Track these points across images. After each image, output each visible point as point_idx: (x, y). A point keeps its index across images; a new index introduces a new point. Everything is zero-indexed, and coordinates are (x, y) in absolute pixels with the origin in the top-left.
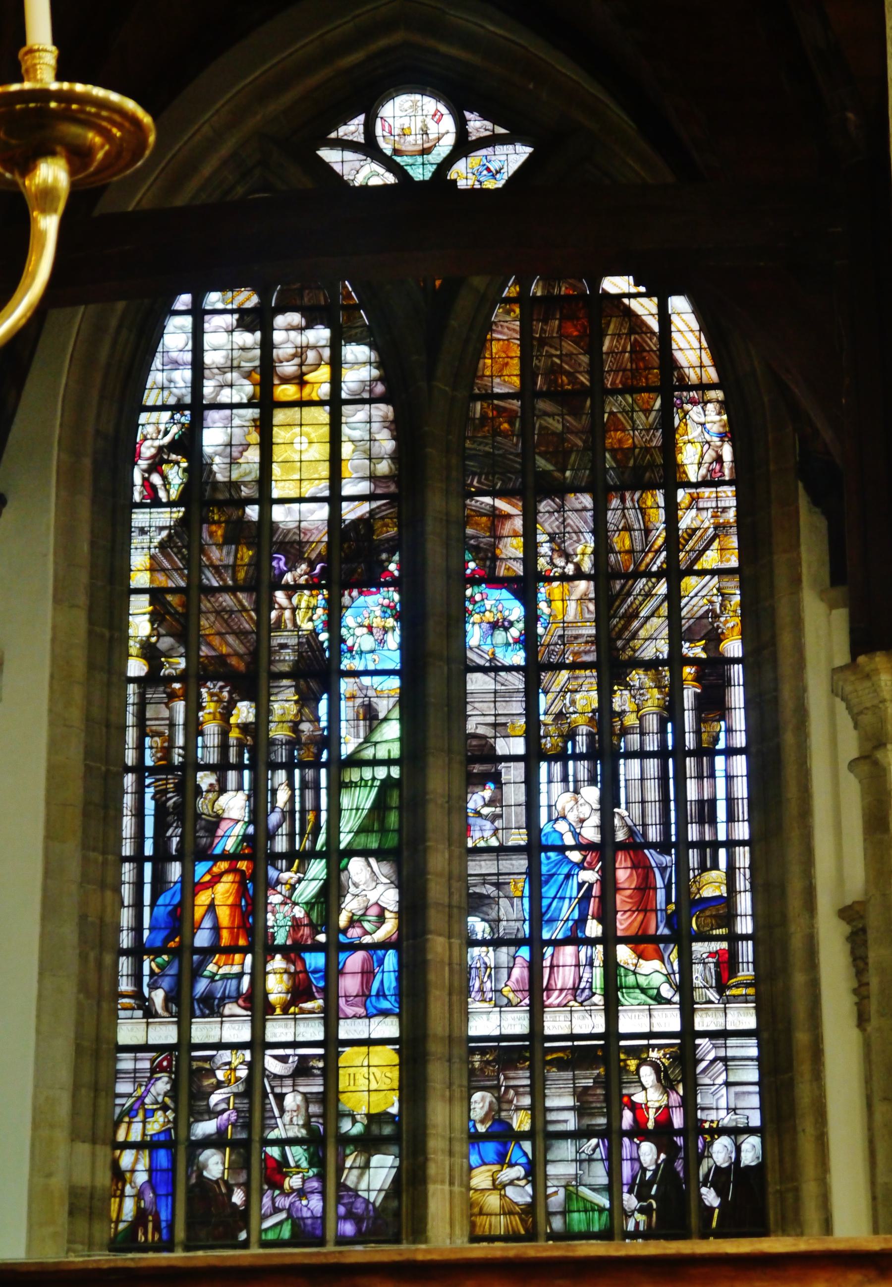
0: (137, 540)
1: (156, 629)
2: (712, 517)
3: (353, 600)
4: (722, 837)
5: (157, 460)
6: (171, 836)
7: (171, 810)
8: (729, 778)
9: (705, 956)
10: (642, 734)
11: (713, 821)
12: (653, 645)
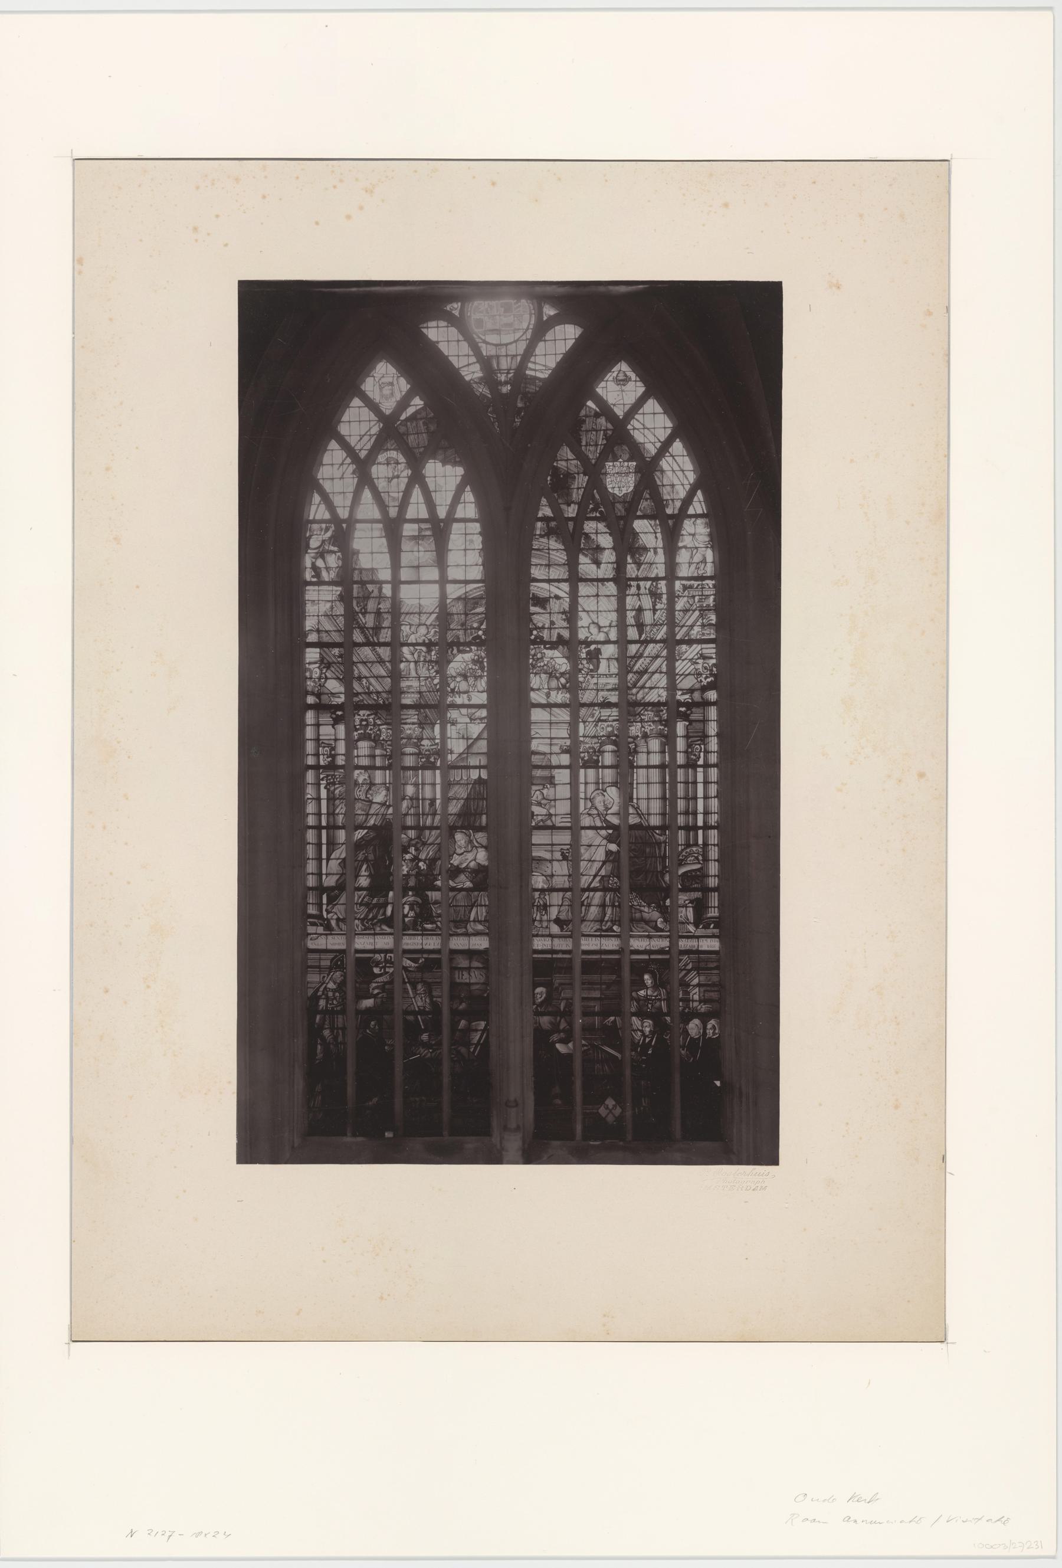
0: (310, 609)
1: (325, 673)
2: (699, 602)
3: (454, 656)
4: (700, 823)
5: (321, 550)
6: (338, 814)
7: (338, 796)
8: (706, 783)
9: (687, 902)
10: (648, 753)
11: (695, 814)
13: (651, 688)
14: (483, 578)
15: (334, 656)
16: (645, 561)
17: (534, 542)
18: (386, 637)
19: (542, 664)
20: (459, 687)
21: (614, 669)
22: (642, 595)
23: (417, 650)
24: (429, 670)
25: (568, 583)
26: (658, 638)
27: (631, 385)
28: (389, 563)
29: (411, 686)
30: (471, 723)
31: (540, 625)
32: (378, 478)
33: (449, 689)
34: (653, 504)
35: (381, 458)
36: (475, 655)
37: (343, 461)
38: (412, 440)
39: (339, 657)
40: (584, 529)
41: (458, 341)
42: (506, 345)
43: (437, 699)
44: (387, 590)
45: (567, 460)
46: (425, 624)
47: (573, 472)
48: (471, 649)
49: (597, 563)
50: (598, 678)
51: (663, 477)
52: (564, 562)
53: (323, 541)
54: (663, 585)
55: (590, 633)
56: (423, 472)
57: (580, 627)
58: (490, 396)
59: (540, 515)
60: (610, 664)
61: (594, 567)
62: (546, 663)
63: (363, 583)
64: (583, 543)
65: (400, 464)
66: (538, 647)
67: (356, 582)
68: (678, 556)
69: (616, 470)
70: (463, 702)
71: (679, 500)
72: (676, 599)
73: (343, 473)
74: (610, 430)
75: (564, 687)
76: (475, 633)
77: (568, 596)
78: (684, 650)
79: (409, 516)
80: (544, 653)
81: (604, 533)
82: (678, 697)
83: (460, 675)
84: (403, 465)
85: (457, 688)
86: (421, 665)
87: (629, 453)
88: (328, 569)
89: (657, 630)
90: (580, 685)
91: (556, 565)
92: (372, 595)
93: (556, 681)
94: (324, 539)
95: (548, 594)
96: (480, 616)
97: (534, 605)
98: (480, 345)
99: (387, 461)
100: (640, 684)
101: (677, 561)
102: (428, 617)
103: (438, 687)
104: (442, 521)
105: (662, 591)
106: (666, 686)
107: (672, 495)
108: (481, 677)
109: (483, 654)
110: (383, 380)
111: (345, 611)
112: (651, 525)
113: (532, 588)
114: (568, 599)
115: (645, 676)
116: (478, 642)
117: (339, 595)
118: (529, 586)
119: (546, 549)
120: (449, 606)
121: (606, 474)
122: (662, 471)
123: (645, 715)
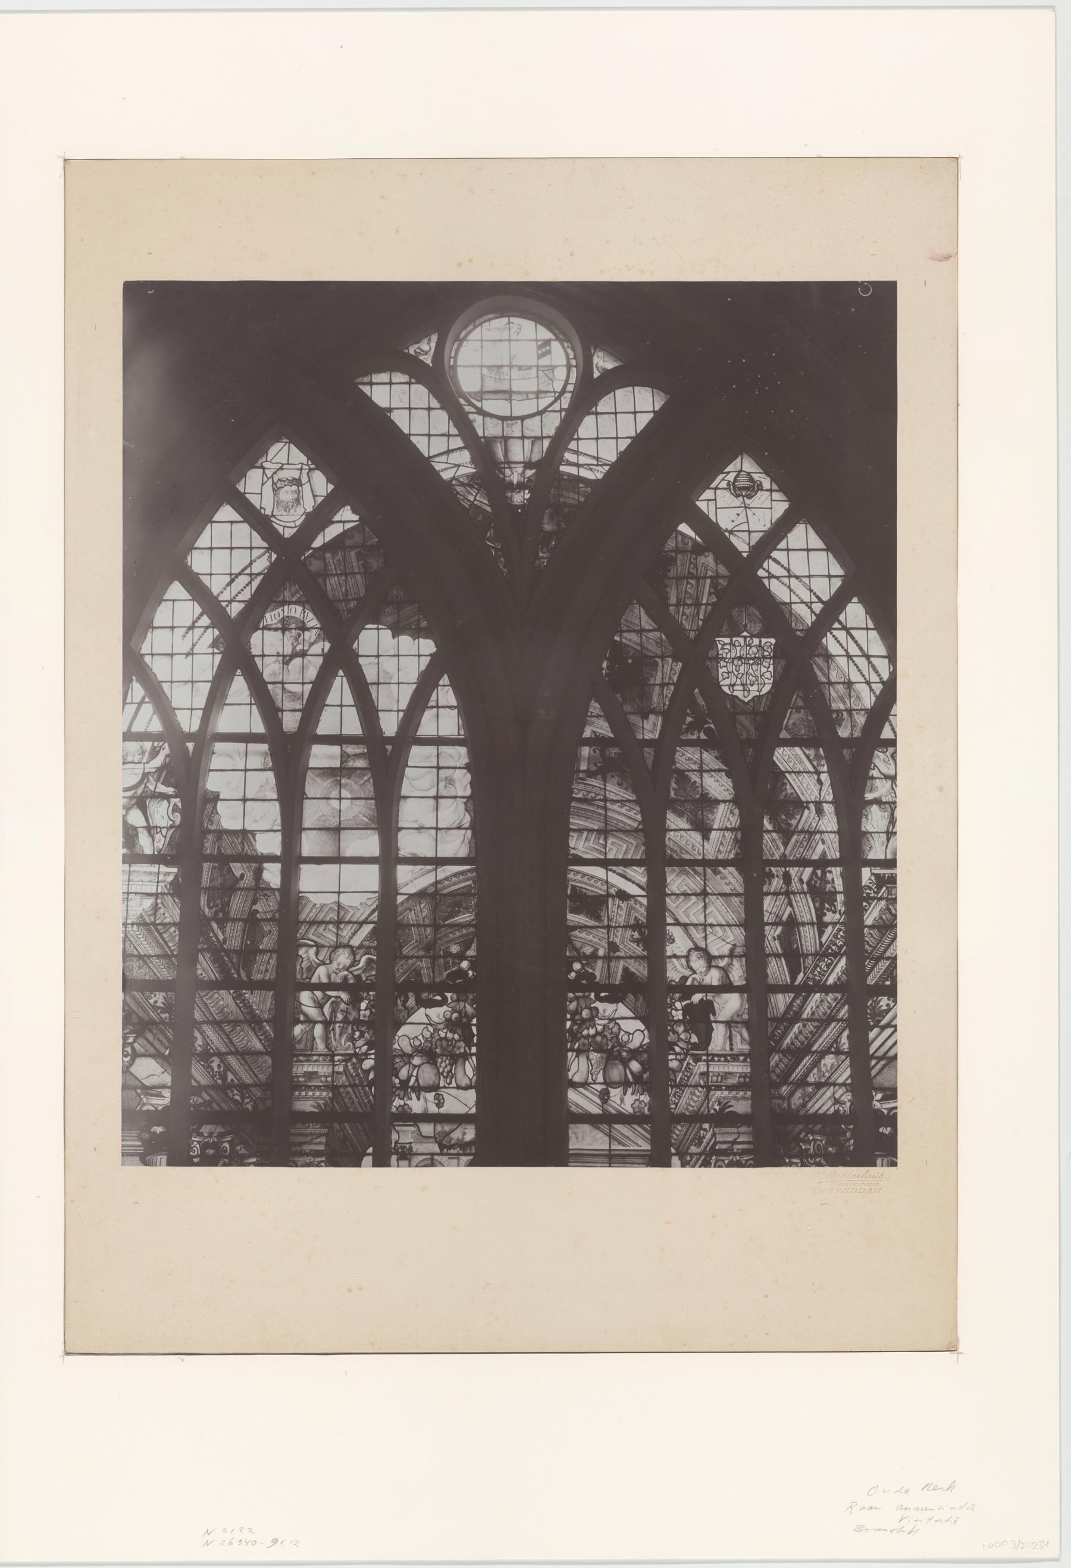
1: (132, 1044)
3: (410, 1012)
12: (829, 1093)
13: (818, 1086)
14: (473, 855)
15: (155, 1007)
16: (800, 827)
17: (575, 786)
18: (267, 970)
19: (592, 1031)
20: (417, 1077)
21: (741, 1046)
22: (794, 893)
23: (330, 997)
24: (352, 1039)
25: (643, 868)
26: (831, 981)
27: (761, 498)
28: (279, 821)
29: (316, 1073)
30: (441, 1154)
31: (588, 950)
32: (263, 656)
33: (397, 1081)
34: (810, 718)
35: (271, 617)
36: (453, 1011)
37: (194, 622)
38: (333, 585)
39: (164, 1011)
40: (674, 763)
41: (429, 409)
42: (523, 418)
43: (370, 1101)
44: (272, 875)
45: (641, 631)
46: (347, 946)
47: (652, 655)
48: (445, 998)
49: (705, 830)
50: (707, 1061)
51: (829, 668)
52: (635, 825)
53: (145, 775)
54: (835, 875)
55: (691, 969)
56: (355, 646)
57: (670, 957)
58: (489, 509)
59: (587, 733)
60: (734, 1033)
61: (696, 837)
62: (599, 1028)
63: (223, 861)
64: (674, 789)
65: (308, 629)
66: (584, 997)
67: (210, 858)
68: (864, 819)
69: (737, 652)
70: (426, 1108)
71: (863, 712)
72: (864, 904)
73: (194, 645)
74: (723, 577)
75: (638, 1078)
76: (454, 965)
77: (644, 893)
78: (884, 1008)
79: (321, 730)
80: (597, 1009)
81: (715, 771)
82: (877, 1105)
83: (419, 1051)
84: (314, 631)
85: (413, 1079)
86: (337, 1030)
87: (761, 621)
88: (150, 829)
89: (828, 966)
90: (672, 1077)
91: (619, 830)
92: (242, 884)
93: (621, 1067)
94: (146, 771)
95: (605, 888)
96: (464, 931)
97: (574, 911)
98: (471, 416)
99: (283, 625)
100: (795, 1076)
101: (863, 829)
102: (356, 932)
103: (371, 1076)
104: (389, 740)
105: (834, 888)
106: (849, 1081)
107: (848, 702)
108: (465, 1056)
109: (469, 1009)
110: (282, 474)
111: (181, 916)
112: (808, 757)
113: (571, 876)
114: (646, 899)
115: (807, 1059)
116: (459, 985)
117: (172, 883)
118: (566, 872)
119: (600, 800)
120: (400, 909)
121: (717, 659)
122: (828, 657)
123: (809, 1142)
